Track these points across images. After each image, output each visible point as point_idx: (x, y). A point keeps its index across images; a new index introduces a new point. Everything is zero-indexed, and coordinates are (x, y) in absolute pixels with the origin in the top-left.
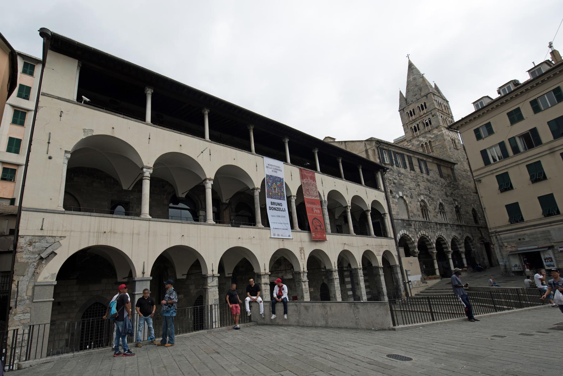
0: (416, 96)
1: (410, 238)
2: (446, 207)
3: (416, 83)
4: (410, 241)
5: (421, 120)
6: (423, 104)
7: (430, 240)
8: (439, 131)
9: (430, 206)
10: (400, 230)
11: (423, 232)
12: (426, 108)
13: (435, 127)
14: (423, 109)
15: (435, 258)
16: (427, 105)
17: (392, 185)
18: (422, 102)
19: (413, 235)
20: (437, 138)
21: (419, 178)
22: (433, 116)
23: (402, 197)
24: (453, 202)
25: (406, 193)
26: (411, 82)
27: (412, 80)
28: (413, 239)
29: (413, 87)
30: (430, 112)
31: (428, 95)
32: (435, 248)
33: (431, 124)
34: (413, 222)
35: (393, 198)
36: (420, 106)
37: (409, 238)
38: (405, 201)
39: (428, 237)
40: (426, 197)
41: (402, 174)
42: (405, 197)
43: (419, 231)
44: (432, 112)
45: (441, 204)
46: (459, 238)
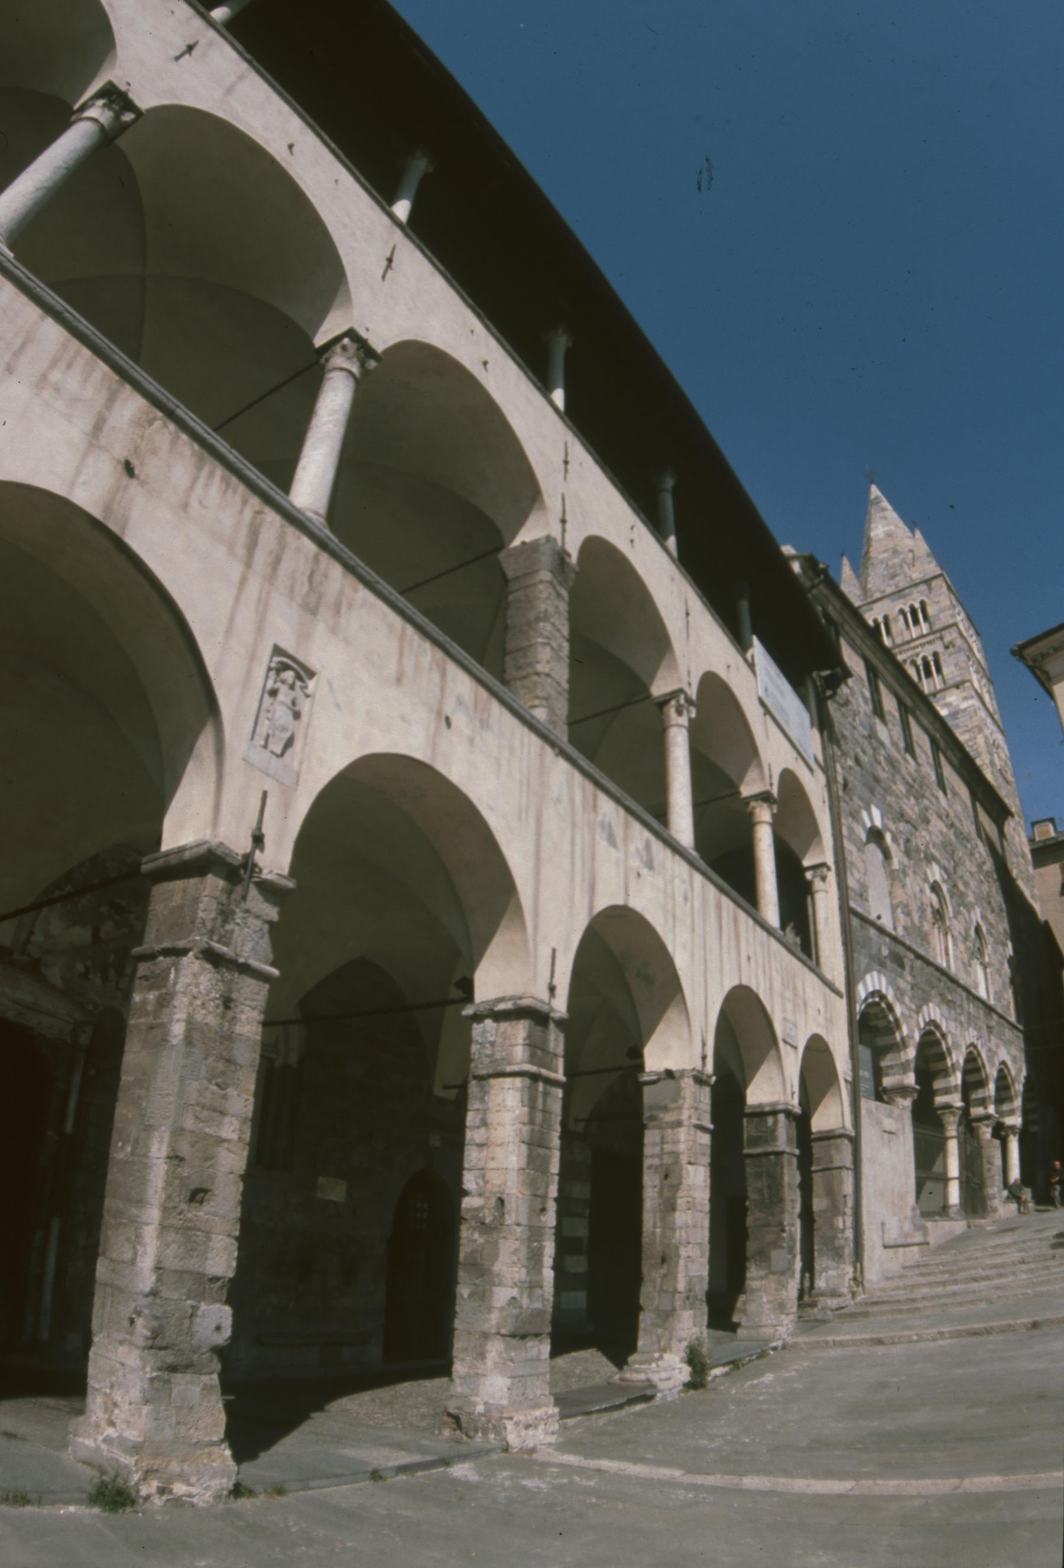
0: (897, 579)
1: (897, 1021)
2: (989, 947)
3: (896, 545)
4: (893, 1033)
5: (910, 653)
6: (917, 605)
7: (950, 1054)
8: (965, 699)
9: (955, 917)
10: (868, 970)
11: (934, 1011)
12: (926, 618)
13: (950, 682)
14: (916, 622)
15: (954, 1133)
16: (931, 610)
17: (850, 762)
18: (915, 600)
19: (906, 1012)
20: (958, 721)
21: (927, 794)
22: (947, 647)
23: (875, 835)
24: (1002, 938)
25: (892, 827)
26: (879, 540)
27: (881, 536)
28: (905, 1030)
29: (886, 555)
30: (938, 635)
31: (934, 584)
32: (960, 1089)
33: (939, 670)
34: (911, 956)
35: (850, 819)
36: (907, 609)
37: (891, 1018)
38: (887, 855)
39: (944, 1036)
40: (946, 877)
41: (882, 744)
42: (888, 837)
43: (926, 1001)
44: (943, 633)
45: (978, 930)
46: (1013, 1073)
